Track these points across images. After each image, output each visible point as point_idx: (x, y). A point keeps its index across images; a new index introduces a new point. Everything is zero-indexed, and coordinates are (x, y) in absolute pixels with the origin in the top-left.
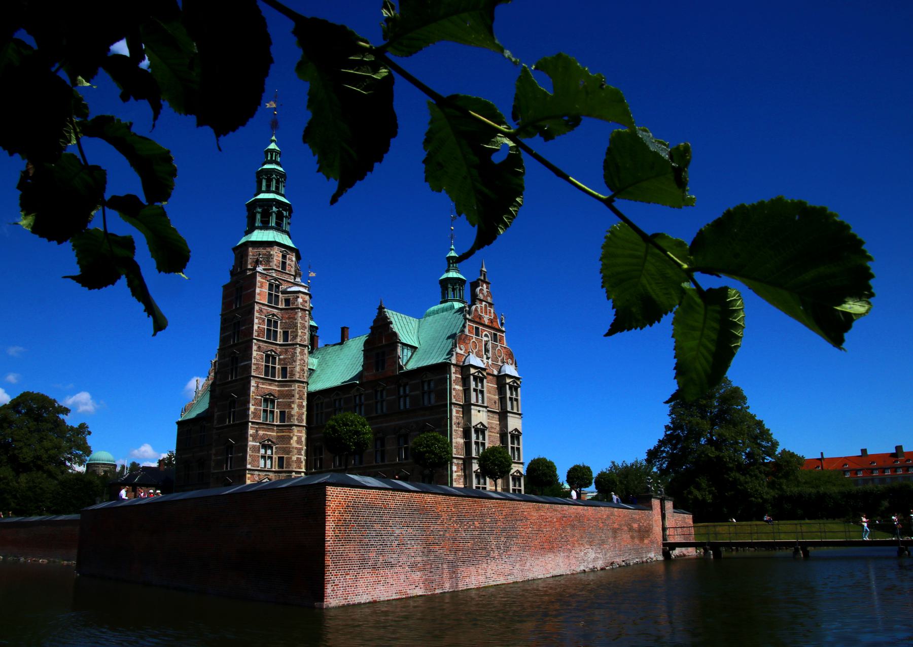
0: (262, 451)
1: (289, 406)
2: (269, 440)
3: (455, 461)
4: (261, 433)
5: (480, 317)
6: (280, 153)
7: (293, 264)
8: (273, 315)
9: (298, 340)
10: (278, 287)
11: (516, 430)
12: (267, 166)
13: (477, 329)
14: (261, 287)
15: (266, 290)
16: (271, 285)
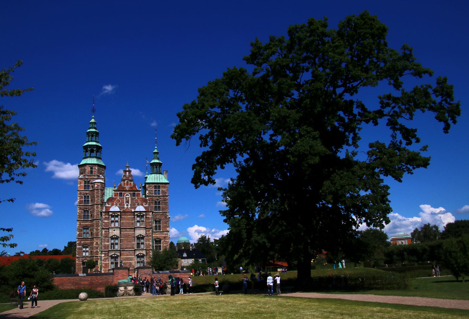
0: (84, 249)
1: (93, 230)
2: (86, 245)
3: (103, 252)
4: (82, 242)
5: (124, 188)
6: (95, 123)
7: (96, 170)
8: (87, 194)
9: (95, 203)
10: (89, 181)
11: (140, 235)
12: (88, 131)
13: (121, 194)
14: (81, 183)
15: (83, 185)
16: (85, 182)
